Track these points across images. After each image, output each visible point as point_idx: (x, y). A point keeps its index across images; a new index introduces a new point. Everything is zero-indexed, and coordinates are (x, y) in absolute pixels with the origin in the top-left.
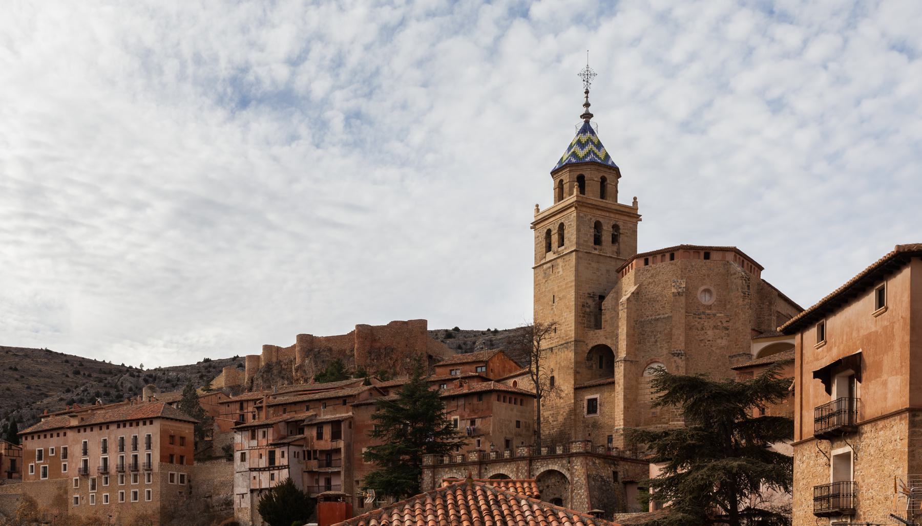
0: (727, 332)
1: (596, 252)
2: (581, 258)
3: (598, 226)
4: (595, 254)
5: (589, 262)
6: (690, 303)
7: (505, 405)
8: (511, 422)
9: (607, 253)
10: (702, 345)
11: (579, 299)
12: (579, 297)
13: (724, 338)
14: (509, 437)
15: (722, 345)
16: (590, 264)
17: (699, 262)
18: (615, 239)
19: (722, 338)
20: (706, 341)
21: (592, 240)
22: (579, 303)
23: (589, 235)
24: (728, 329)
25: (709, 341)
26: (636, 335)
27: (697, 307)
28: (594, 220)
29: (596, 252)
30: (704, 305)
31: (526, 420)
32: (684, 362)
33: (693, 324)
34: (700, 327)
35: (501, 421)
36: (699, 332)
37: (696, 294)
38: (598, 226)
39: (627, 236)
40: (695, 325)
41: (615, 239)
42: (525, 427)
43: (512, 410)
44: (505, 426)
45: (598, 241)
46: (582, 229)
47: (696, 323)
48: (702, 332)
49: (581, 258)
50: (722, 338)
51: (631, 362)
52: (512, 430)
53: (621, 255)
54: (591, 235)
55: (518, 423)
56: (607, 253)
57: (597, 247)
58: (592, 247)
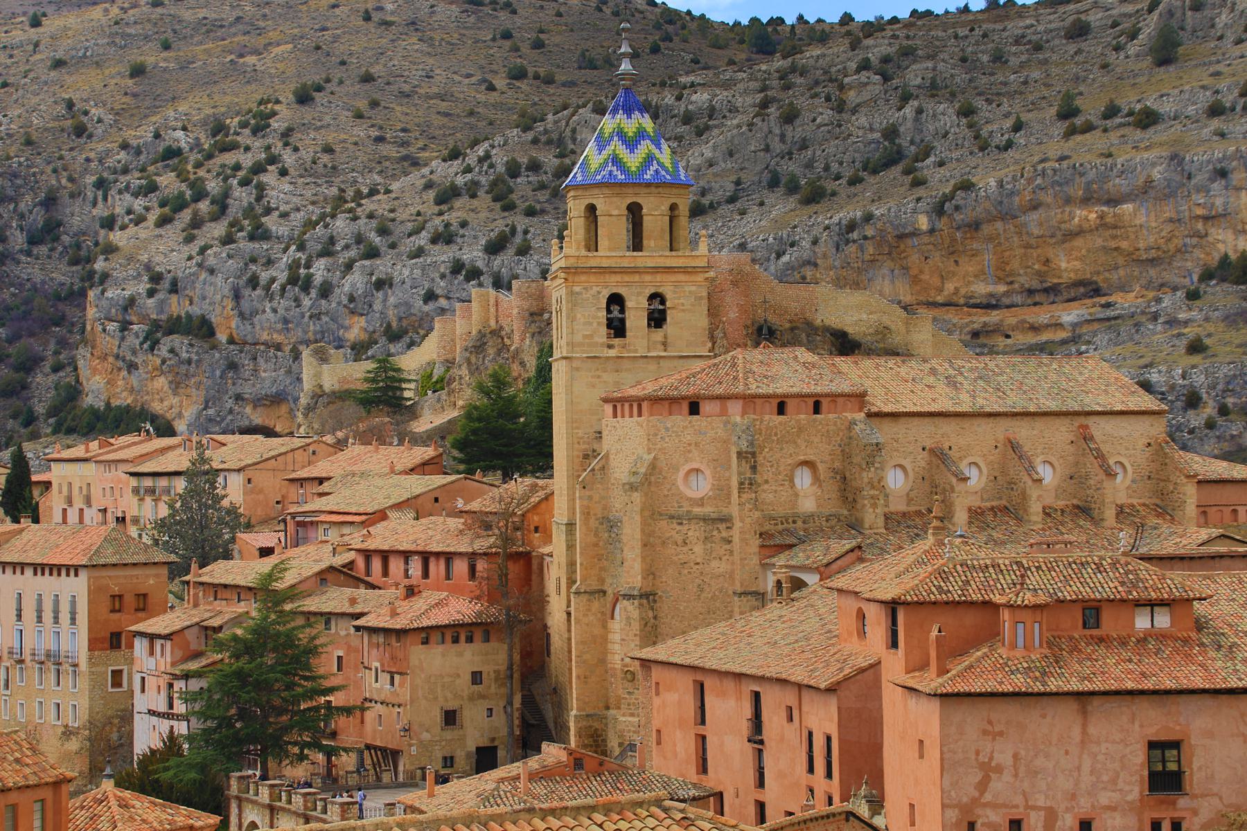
0: (728, 547)
1: (612, 353)
2: (577, 369)
3: (616, 300)
4: (608, 358)
5: (598, 373)
6: (666, 496)
7: (440, 648)
8: (458, 676)
9: (636, 351)
10: (686, 571)
11: (576, 446)
12: (576, 442)
13: (724, 558)
14: (451, 705)
15: (721, 570)
16: (599, 377)
17: (680, 420)
18: (657, 319)
19: (720, 559)
20: (692, 564)
21: (604, 330)
22: (576, 453)
23: (595, 324)
24: (730, 542)
25: (698, 564)
26: (601, 544)
27: (678, 503)
28: (606, 293)
29: (612, 353)
30: (691, 499)
31: (496, 668)
32: (638, 611)
33: (668, 535)
34: (679, 539)
35: (433, 679)
36: (679, 549)
37: (675, 479)
38: (616, 300)
39: (683, 310)
40: (671, 537)
41: (657, 319)
42: (496, 679)
43: (460, 654)
44: (443, 686)
45: (617, 328)
46: (579, 316)
47: (673, 533)
48: (685, 549)
49: (577, 369)
50: (720, 559)
51: (592, 593)
52: (463, 690)
53: (669, 349)
54: (599, 323)
55: (476, 677)
56: (636, 351)
57: (617, 341)
58: (602, 345)
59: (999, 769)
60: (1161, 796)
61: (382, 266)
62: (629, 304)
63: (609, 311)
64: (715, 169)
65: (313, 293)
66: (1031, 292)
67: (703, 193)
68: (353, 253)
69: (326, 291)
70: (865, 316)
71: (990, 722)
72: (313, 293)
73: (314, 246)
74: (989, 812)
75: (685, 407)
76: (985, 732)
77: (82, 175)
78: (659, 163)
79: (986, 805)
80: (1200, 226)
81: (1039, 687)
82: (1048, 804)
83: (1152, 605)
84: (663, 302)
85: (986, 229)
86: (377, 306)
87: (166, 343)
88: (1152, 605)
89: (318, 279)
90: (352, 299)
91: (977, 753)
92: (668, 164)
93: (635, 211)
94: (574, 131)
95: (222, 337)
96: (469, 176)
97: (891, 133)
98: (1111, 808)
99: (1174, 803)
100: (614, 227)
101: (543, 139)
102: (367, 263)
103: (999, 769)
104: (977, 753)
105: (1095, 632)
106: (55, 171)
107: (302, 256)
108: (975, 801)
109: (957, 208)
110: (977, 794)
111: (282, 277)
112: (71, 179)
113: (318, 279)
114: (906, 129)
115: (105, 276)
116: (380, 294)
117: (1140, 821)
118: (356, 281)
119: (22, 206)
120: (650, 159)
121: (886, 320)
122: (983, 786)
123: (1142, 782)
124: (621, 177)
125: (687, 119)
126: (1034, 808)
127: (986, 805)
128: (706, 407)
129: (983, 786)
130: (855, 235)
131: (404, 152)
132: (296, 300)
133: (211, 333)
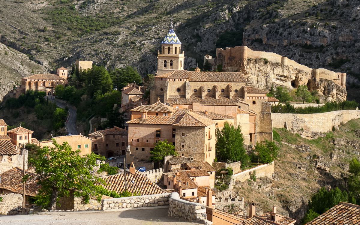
1: (164, 69)
3: (165, 61)
18: (171, 64)
38: (165, 61)
41: (171, 64)
45: (165, 66)
59: (136, 133)
60: (157, 138)
61: (291, 30)
63: (164, 63)
64: (359, 11)
65: (279, 35)
67: (357, 16)
68: (288, 27)
69: (281, 34)
70: (272, 57)
72: (279, 35)
73: (281, 25)
75: (161, 79)
77: (255, 7)
81: (141, 123)
83: (166, 113)
86: (289, 38)
87: (254, 44)
88: (166, 113)
89: (280, 32)
90: (285, 37)
92: (176, 41)
94: (336, 2)
95: (264, 43)
96: (313, 11)
98: (151, 139)
100: (166, 51)
101: (330, 3)
102: (288, 29)
103: (136, 133)
105: (157, 116)
106: (250, 6)
107: (279, 27)
111: (275, 31)
112: (253, 8)
113: (280, 32)
115: (246, 30)
116: (289, 36)
118: (286, 33)
119: (243, 14)
120: (172, 40)
121: (277, 58)
124: (167, 43)
128: (163, 79)
131: (309, 4)
132: (276, 36)
133: (262, 42)
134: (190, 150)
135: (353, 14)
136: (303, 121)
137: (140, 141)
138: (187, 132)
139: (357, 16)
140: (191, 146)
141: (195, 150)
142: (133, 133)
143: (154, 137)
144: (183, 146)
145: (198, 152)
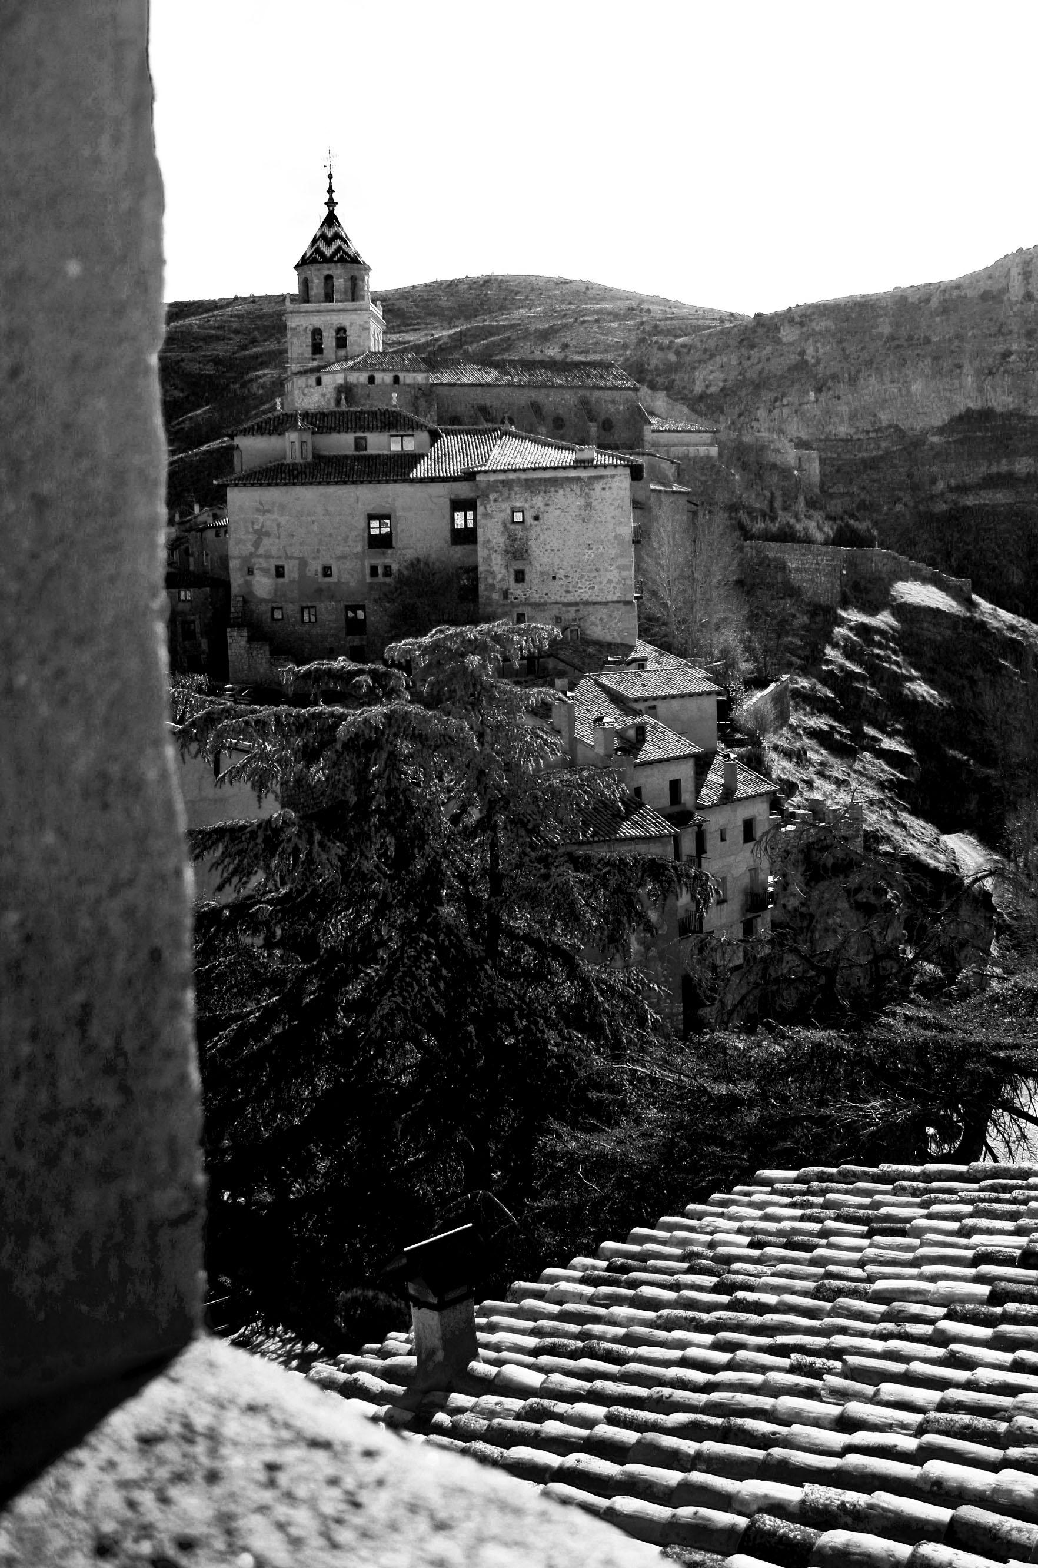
21: (310, 349)
38: (317, 333)
57: (317, 356)
59: (268, 534)
62: (325, 334)
63: (314, 339)
66: (868, 432)
67: (707, 387)
71: (261, 504)
74: (261, 560)
76: (258, 510)
78: (344, 252)
79: (260, 556)
80: (948, 394)
82: (301, 555)
84: (345, 331)
85: (844, 399)
91: (253, 523)
93: (329, 278)
97: (802, 353)
99: (384, 554)
103: (268, 534)
104: (253, 523)
108: (251, 554)
109: (829, 389)
110: (253, 550)
114: (810, 350)
117: (363, 565)
122: (257, 544)
123: (363, 540)
125: (705, 350)
126: (291, 558)
127: (260, 556)
129: (257, 544)
130: (778, 404)
134: (556, 592)
135: (698, 383)
136: (782, 567)
137: (292, 570)
138: (538, 501)
139: (707, 387)
140: (561, 573)
141: (585, 593)
142: (252, 537)
143: (359, 548)
144: (520, 576)
145: (599, 599)
